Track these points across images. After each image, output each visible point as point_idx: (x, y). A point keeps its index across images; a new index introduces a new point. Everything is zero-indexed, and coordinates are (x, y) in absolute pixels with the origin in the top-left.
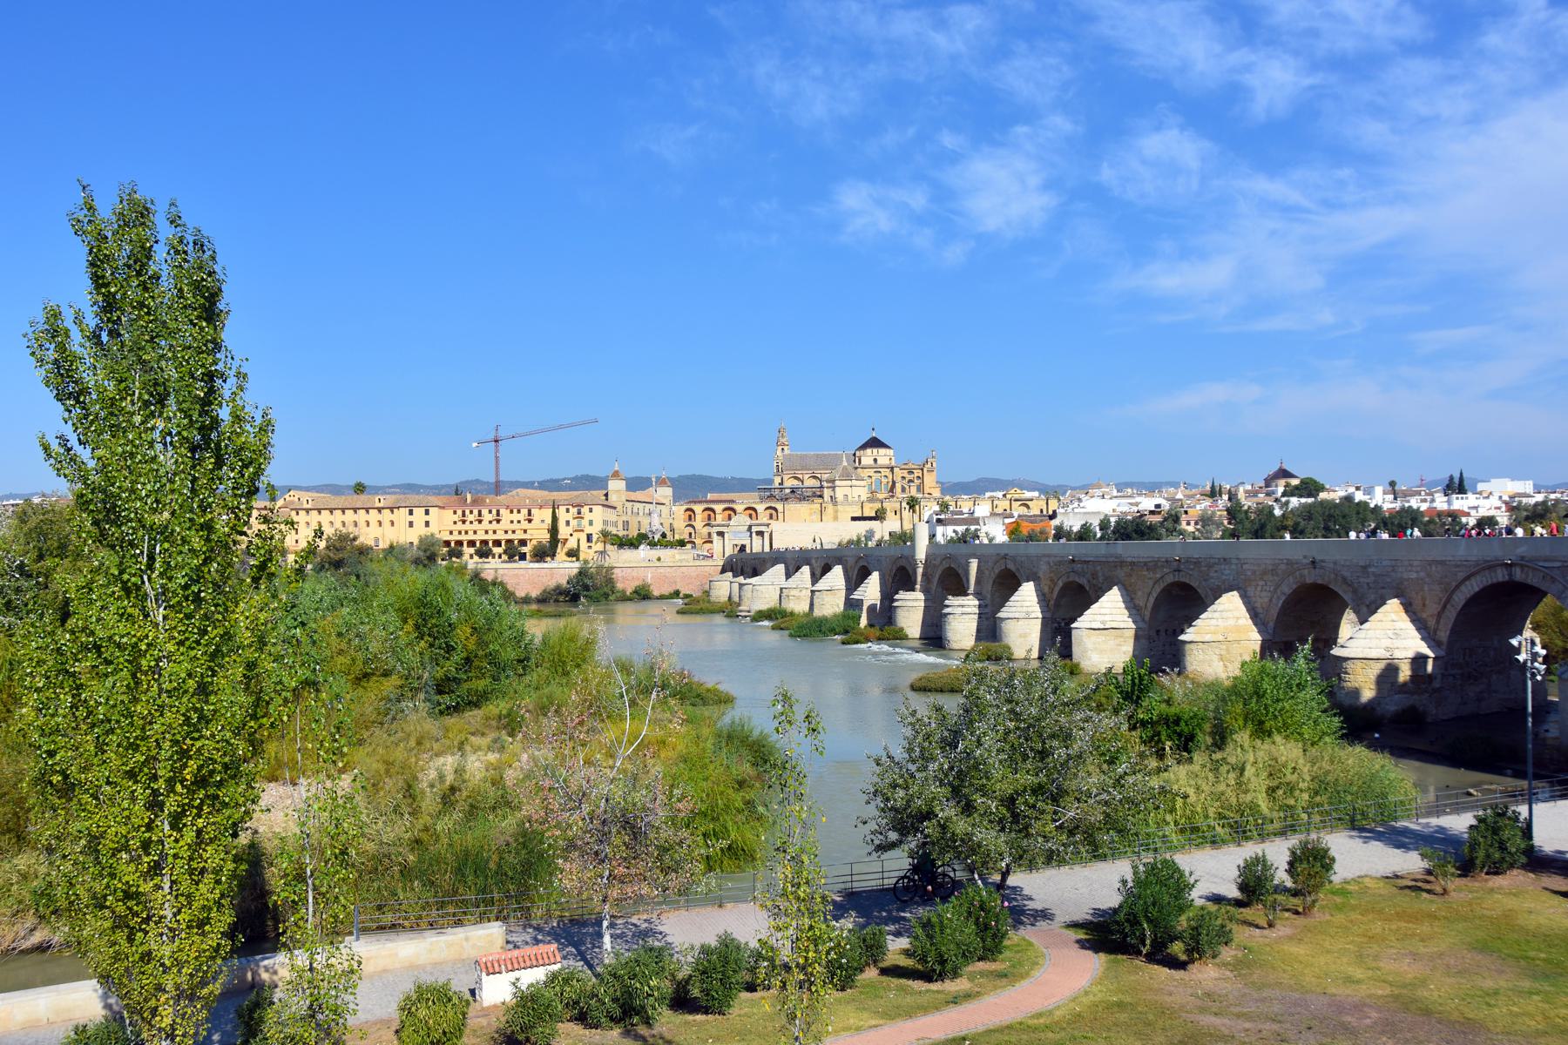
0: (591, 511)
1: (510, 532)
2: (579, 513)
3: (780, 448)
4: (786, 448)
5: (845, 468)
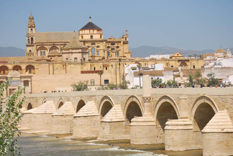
3: (30, 29)
4: (33, 29)
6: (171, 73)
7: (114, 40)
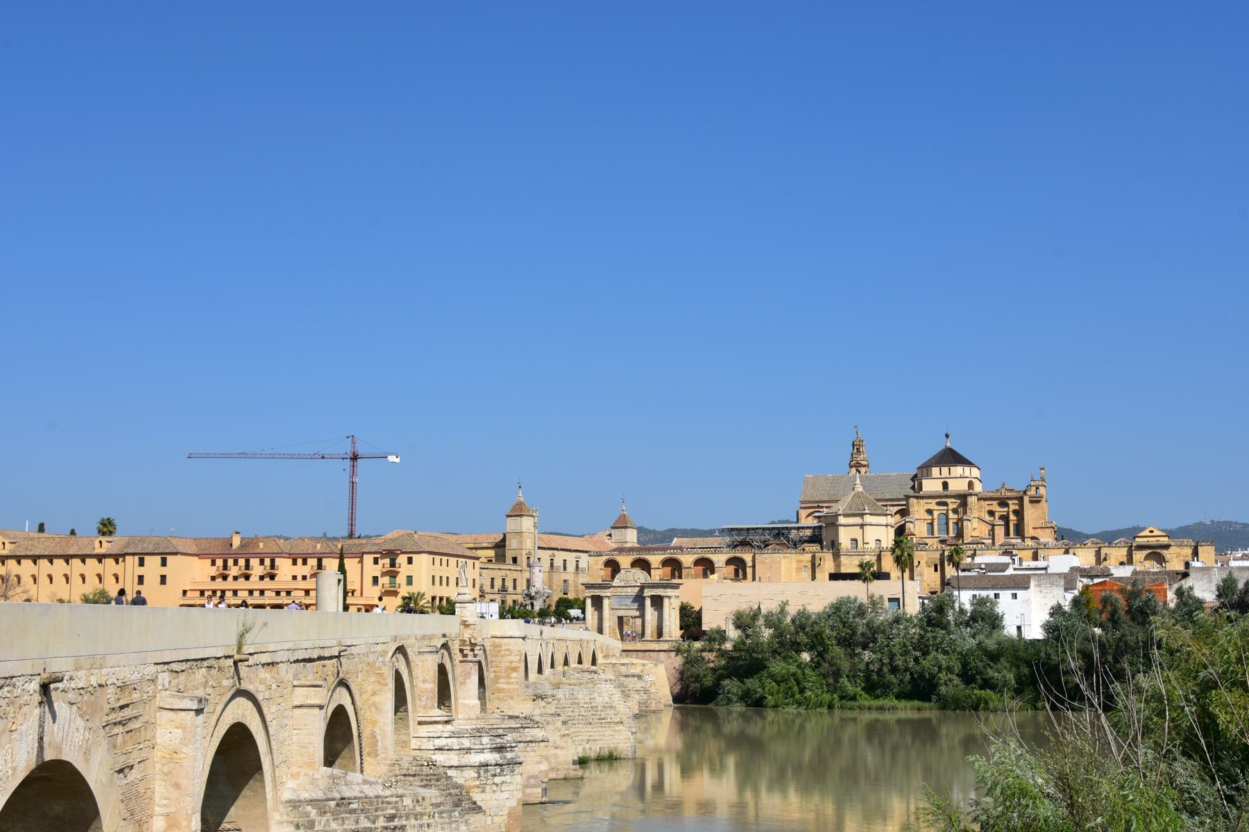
0: (410, 561)
1: (283, 594)
2: (393, 564)
3: (854, 470)
4: (863, 470)
5: (858, 495)
6: (1056, 581)
7: (1008, 494)
